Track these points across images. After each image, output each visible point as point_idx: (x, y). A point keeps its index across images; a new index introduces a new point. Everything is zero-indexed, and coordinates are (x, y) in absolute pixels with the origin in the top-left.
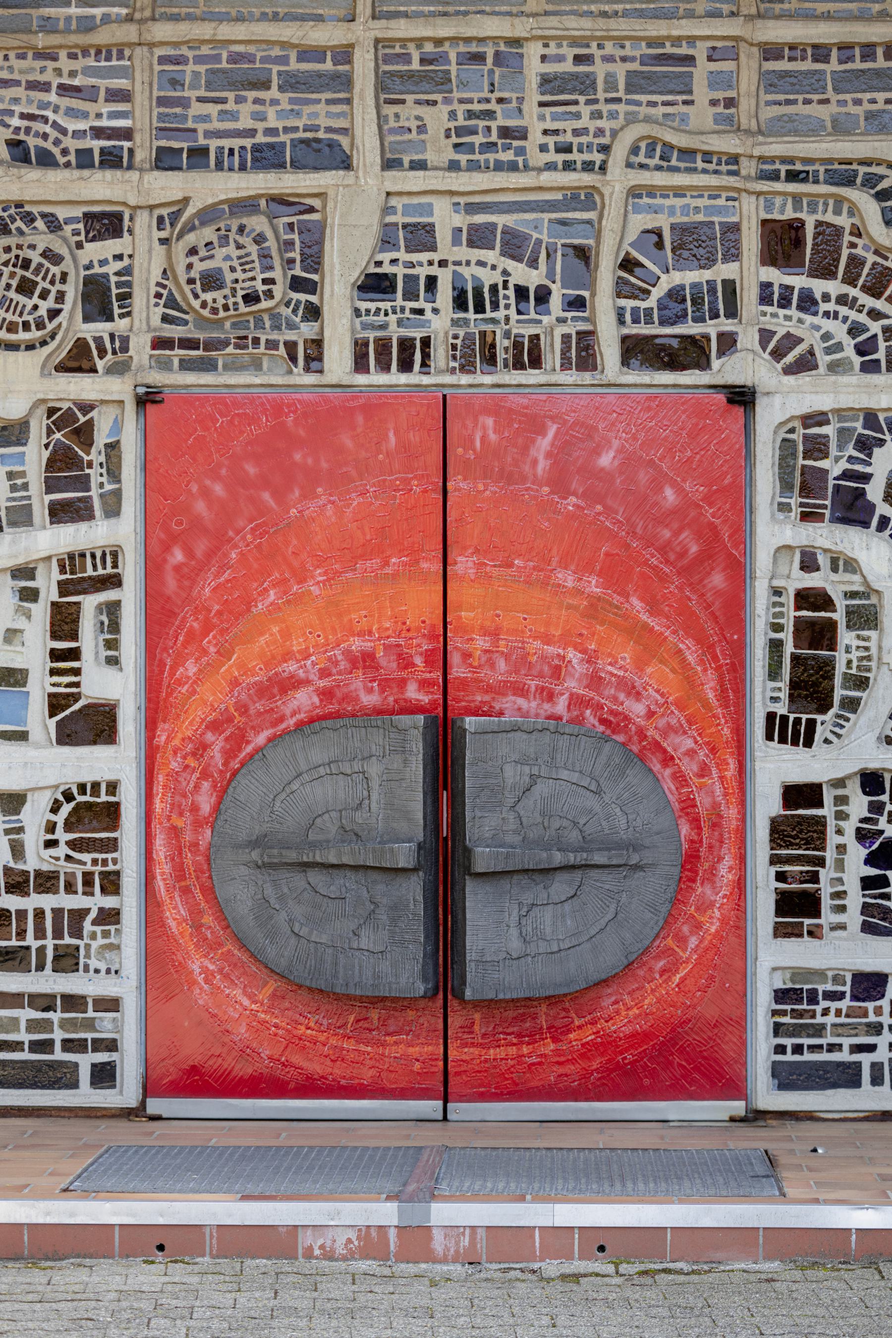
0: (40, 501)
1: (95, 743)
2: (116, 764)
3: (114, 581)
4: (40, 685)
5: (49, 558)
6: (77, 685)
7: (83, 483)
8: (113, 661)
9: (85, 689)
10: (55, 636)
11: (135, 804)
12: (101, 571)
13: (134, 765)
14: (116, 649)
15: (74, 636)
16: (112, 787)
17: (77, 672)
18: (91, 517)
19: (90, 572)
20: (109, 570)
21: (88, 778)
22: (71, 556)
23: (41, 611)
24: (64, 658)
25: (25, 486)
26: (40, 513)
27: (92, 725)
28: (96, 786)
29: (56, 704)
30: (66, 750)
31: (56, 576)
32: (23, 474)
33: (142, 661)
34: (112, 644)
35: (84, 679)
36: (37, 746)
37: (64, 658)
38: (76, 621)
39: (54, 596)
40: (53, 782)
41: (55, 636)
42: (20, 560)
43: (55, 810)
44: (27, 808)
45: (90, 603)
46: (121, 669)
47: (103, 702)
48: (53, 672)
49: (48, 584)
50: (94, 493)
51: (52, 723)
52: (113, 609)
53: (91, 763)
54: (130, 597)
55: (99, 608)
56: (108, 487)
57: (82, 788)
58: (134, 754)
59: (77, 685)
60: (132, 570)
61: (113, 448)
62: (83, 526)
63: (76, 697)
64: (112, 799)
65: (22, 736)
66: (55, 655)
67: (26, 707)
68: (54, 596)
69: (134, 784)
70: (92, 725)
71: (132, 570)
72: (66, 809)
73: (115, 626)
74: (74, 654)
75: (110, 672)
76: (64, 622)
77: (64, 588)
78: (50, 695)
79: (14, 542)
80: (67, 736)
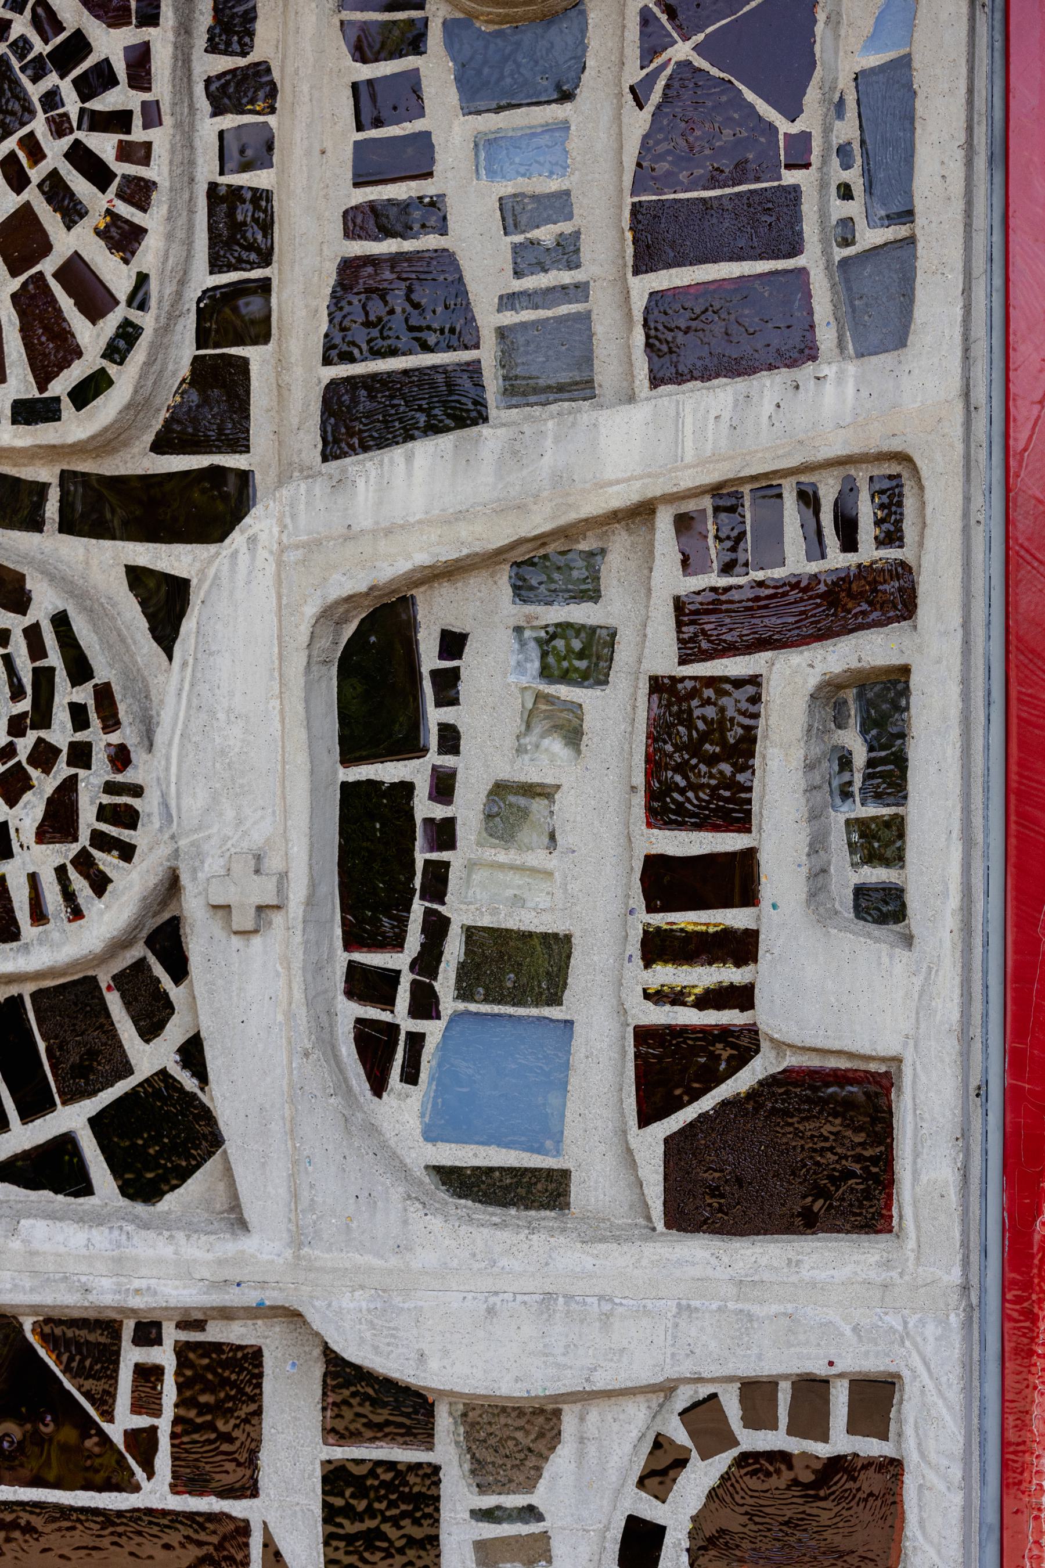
0: (615, 298)
1: (808, 1223)
2: (888, 1306)
3: (885, 596)
4: (608, 1000)
5: (642, 512)
6: (741, 997)
7: (773, 225)
8: (883, 907)
9: (769, 1015)
10: (662, 810)
11: (956, 1473)
12: (837, 559)
13: (955, 1320)
14: (898, 859)
15: (734, 811)
16: (875, 1399)
17: (742, 947)
18: (808, 352)
19: (796, 561)
20: (868, 552)
21: (780, 1360)
22: (725, 497)
23: (616, 716)
24: (697, 895)
25: (567, 252)
26: (618, 345)
27: (785, 1154)
28: (811, 1390)
29: (666, 1068)
30: (701, 1254)
31: (670, 580)
32: (560, 204)
33: (991, 909)
34: (881, 842)
35: (765, 975)
36: (599, 1232)
37: (697, 895)
38: (744, 750)
39: (663, 658)
40: (643, 1370)
41: (662, 810)
42: (539, 521)
43: (661, 1471)
44: (561, 1463)
45: (791, 679)
46: (908, 940)
47: (843, 1064)
48: (657, 947)
49: (640, 608)
50: (812, 258)
51: (651, 1143)
52: (881, 702)
53: (797, 1303)
54: (944, 659)
55: (830, 696)
56: (869, 237)
57: (757, 1394)
58: (955, 1276)
59: (741, 997)
60: (950, 551)
61: (888, 96)
62: (769, 387)
63: (743, 1045)
64: (871, 1447)
65: (537, 1191)
66: (666, 882)
67: (558, 1080)
68: (663, 658)
69: (954, 1395)
70: (785, 1154)
71: (950, 551)
72: (698, 1479)
73: (890, 774)
74: (734, 879)
75: (867, 948)
76: (697, 759)
77: (699, 625)
78: (644, 1035)
79: (514, 453)
80: (708, 1194)
